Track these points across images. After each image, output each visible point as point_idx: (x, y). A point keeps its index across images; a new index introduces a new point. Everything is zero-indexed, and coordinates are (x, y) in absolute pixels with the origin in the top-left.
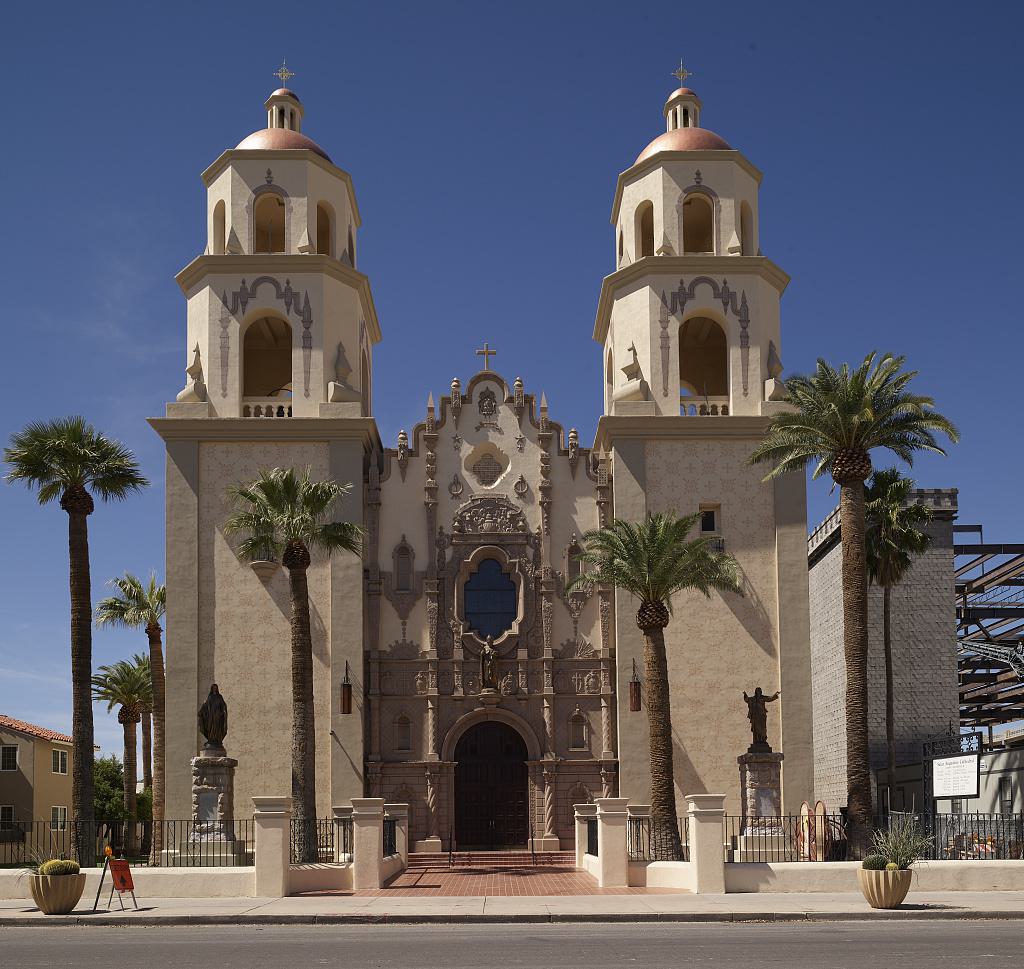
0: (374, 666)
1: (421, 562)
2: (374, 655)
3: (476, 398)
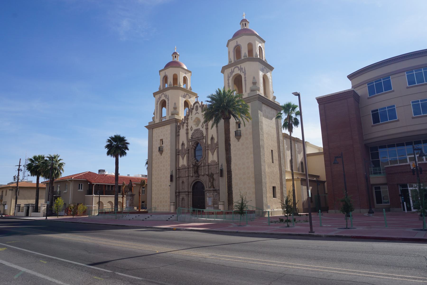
0: (178, 171)
1: (186, 147)
2: (178, 168)
3: (195, 108)
